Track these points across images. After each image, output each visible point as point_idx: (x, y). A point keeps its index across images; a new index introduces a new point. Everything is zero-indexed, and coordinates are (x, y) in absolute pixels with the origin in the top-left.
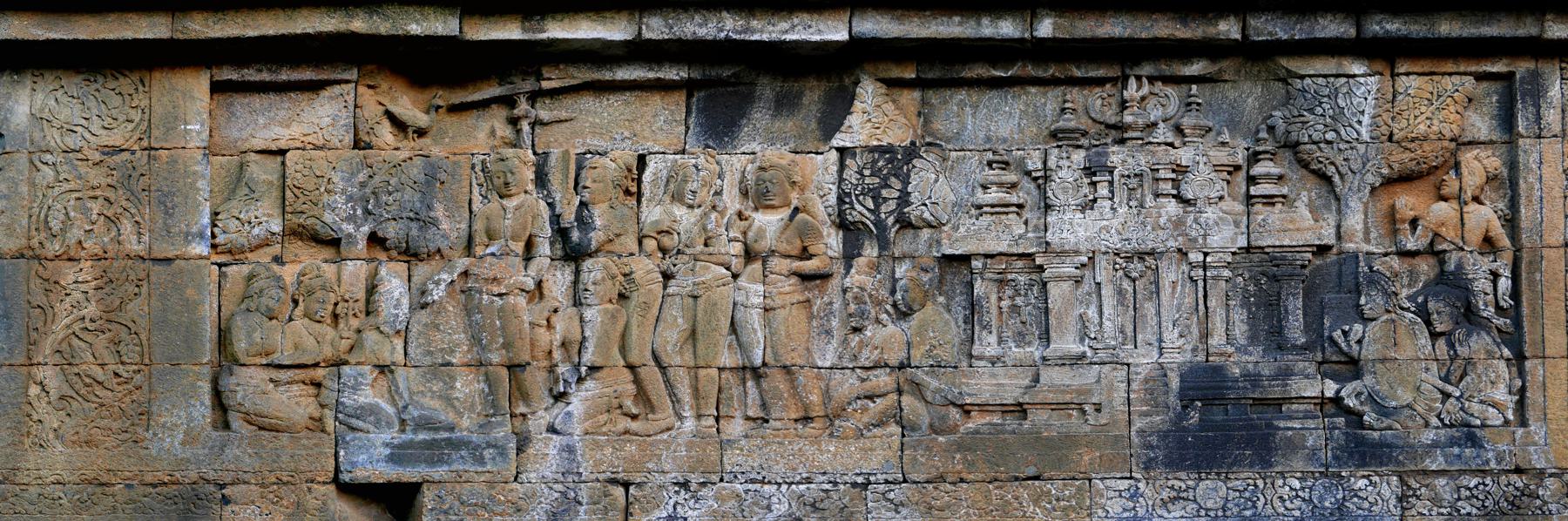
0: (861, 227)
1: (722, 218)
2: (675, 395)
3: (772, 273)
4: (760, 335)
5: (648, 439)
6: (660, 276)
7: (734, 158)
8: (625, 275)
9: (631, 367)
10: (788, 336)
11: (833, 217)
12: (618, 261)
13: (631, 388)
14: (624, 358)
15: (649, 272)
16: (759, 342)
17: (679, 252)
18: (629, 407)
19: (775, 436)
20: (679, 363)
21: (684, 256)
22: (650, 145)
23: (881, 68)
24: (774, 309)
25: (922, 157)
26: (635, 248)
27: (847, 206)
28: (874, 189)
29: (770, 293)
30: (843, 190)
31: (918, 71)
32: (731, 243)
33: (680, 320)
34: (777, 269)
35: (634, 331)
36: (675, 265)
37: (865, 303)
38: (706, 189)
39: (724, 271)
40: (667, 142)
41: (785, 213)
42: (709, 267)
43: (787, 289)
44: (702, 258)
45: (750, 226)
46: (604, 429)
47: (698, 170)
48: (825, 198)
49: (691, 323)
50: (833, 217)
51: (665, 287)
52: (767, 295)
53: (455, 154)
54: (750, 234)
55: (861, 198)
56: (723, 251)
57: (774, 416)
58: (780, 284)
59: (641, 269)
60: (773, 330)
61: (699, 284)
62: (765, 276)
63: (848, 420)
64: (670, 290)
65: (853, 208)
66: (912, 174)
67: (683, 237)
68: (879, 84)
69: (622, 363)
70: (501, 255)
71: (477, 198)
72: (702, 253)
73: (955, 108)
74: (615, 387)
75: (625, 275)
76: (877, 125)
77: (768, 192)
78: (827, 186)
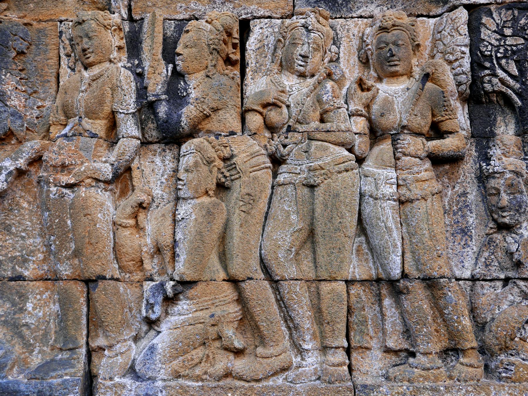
1: (340, 89)
2: (292, 320)
3: (405, 155)
4: (396, 235)
5: (256, 385)
6: (267, 160)
7: (350, 22)
8: (225, 160)
9: (234, 281)
10: (432, 237)
11: (463, 87)
12: (216, 142)
13: (234, 310)
14: (225, 268)
15: (253, 155)
16: (395, 246)
17: (290, 129)
18: (230, 338)
19: (426, 379)
20: (294, 275)
21: (296, 135)
22: (253, 8)
24: (411, 201)
26: (237, 126)
27: (487, 72)
28: (519, 51)
29: (404, 180)
30: (481, 52)
32: (353, 118)
33: (293, 217)
34: (411, 150)
35: (236, 233)
36: (285, 146)
37: (521, 193)
38: (319, 55)
39: (346, 153)
40: (273, 5)
41: (412, 84)
42: (326, 149)
43: (424, 175)
44: (318, 136)
45: (374, 97)
46: (198, 371)
47: (309, 31)
48: (456, 64)
49: (308, 221)
50: (463, 87)
51: (275, 175)
52: (400, 182)
53: (40, 21)
54: (375, 108)
55: (503, 61)
56: (343, 127)
57: (422, 348)
58: (416, 169)
59: (244, 151)
60: (412, 230)
61: (315, 170)
62: (397, 159)
63: (518, 354)
64: (281, 178)
65: (495, 75)
67: (294, 111)
69: (222, 275)
70: (74, 135)
71: (65, 70)
72: (317, 130)
74: (213, 310)
75: (225, 160)
77: (393, 55)
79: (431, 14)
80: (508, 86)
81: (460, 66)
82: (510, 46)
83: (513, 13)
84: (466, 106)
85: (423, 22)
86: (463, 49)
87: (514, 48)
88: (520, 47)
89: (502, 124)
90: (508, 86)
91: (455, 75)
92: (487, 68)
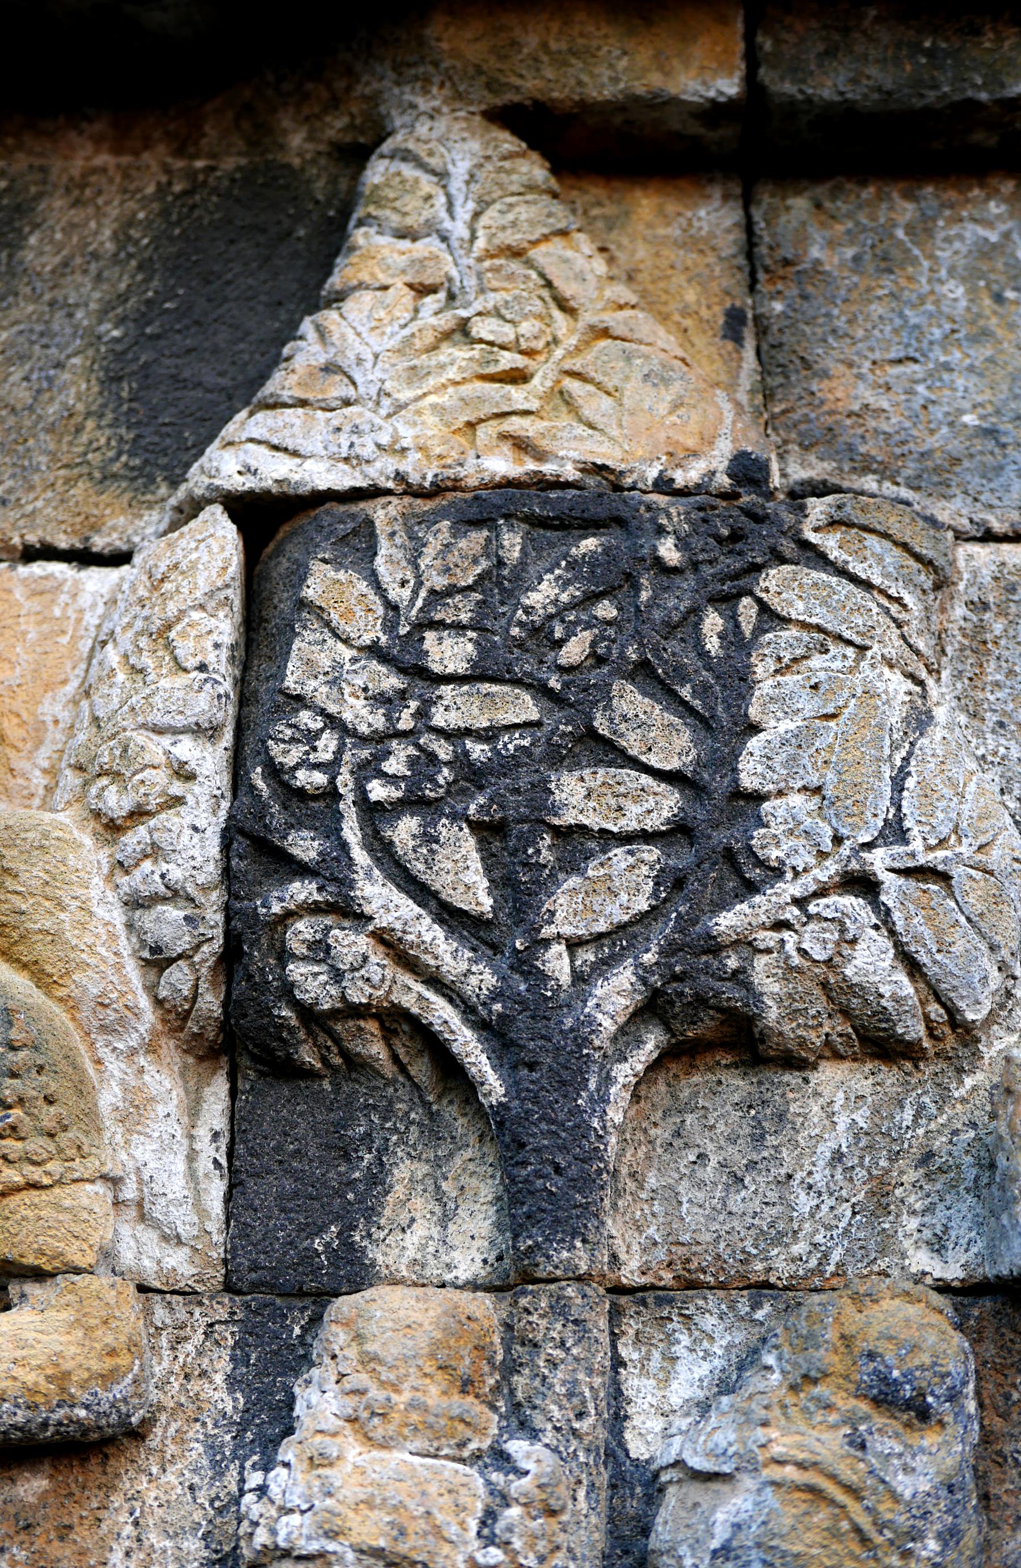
0: (376, 1049)
23: (531, 41)
25: (818, 558)
30: (275, 772)
31: (752, 59)
48: (136, 837)
66: (762, 669)
68: (508, 142)
73: (956, 291)
76: (508, 360)
78: (156, 748)
79: (99, 543)
80: (435, 981)
81: (154, 851)
82: (453, 735)
83: (492, 549)
84: (217, 1091)
85: (38, 591)
86: (186, 749)
87: (478, 751)
88: (511, 743)
89: (421, 1205)
90: (435, 981)
91: (136, 903)
92: (303, 870)
